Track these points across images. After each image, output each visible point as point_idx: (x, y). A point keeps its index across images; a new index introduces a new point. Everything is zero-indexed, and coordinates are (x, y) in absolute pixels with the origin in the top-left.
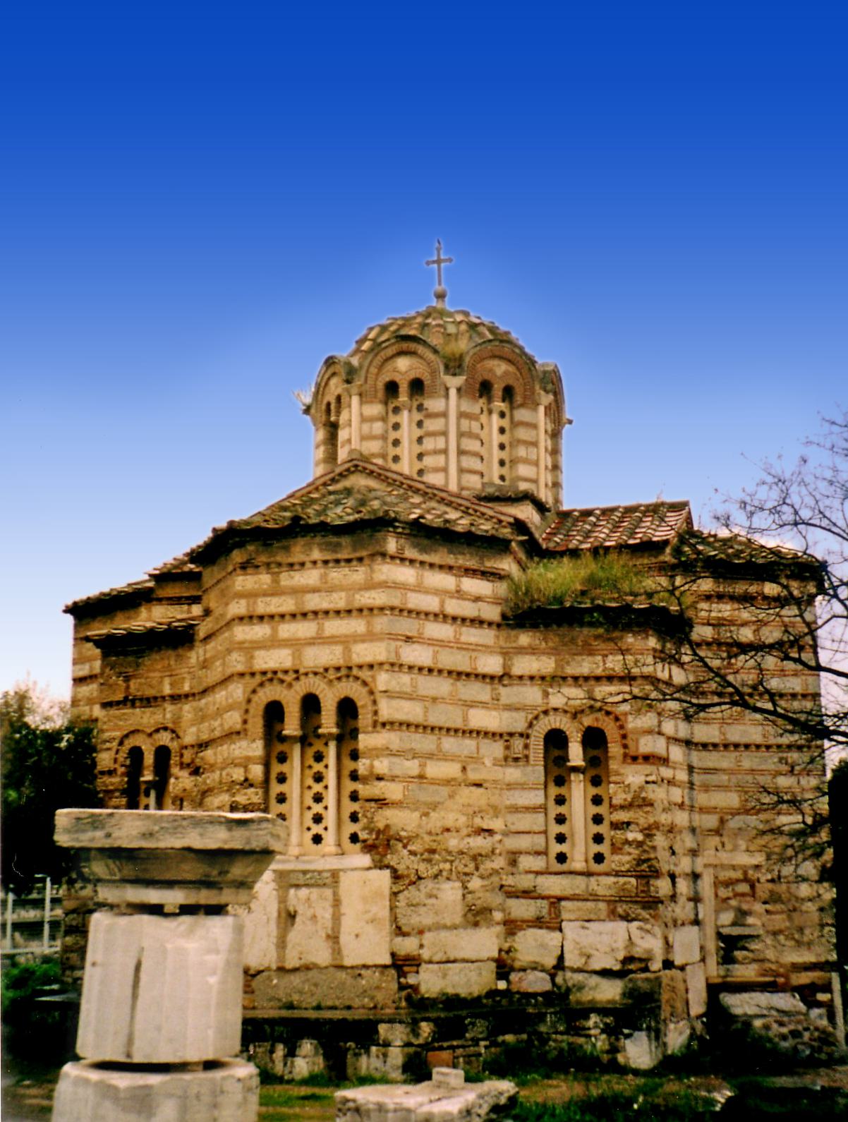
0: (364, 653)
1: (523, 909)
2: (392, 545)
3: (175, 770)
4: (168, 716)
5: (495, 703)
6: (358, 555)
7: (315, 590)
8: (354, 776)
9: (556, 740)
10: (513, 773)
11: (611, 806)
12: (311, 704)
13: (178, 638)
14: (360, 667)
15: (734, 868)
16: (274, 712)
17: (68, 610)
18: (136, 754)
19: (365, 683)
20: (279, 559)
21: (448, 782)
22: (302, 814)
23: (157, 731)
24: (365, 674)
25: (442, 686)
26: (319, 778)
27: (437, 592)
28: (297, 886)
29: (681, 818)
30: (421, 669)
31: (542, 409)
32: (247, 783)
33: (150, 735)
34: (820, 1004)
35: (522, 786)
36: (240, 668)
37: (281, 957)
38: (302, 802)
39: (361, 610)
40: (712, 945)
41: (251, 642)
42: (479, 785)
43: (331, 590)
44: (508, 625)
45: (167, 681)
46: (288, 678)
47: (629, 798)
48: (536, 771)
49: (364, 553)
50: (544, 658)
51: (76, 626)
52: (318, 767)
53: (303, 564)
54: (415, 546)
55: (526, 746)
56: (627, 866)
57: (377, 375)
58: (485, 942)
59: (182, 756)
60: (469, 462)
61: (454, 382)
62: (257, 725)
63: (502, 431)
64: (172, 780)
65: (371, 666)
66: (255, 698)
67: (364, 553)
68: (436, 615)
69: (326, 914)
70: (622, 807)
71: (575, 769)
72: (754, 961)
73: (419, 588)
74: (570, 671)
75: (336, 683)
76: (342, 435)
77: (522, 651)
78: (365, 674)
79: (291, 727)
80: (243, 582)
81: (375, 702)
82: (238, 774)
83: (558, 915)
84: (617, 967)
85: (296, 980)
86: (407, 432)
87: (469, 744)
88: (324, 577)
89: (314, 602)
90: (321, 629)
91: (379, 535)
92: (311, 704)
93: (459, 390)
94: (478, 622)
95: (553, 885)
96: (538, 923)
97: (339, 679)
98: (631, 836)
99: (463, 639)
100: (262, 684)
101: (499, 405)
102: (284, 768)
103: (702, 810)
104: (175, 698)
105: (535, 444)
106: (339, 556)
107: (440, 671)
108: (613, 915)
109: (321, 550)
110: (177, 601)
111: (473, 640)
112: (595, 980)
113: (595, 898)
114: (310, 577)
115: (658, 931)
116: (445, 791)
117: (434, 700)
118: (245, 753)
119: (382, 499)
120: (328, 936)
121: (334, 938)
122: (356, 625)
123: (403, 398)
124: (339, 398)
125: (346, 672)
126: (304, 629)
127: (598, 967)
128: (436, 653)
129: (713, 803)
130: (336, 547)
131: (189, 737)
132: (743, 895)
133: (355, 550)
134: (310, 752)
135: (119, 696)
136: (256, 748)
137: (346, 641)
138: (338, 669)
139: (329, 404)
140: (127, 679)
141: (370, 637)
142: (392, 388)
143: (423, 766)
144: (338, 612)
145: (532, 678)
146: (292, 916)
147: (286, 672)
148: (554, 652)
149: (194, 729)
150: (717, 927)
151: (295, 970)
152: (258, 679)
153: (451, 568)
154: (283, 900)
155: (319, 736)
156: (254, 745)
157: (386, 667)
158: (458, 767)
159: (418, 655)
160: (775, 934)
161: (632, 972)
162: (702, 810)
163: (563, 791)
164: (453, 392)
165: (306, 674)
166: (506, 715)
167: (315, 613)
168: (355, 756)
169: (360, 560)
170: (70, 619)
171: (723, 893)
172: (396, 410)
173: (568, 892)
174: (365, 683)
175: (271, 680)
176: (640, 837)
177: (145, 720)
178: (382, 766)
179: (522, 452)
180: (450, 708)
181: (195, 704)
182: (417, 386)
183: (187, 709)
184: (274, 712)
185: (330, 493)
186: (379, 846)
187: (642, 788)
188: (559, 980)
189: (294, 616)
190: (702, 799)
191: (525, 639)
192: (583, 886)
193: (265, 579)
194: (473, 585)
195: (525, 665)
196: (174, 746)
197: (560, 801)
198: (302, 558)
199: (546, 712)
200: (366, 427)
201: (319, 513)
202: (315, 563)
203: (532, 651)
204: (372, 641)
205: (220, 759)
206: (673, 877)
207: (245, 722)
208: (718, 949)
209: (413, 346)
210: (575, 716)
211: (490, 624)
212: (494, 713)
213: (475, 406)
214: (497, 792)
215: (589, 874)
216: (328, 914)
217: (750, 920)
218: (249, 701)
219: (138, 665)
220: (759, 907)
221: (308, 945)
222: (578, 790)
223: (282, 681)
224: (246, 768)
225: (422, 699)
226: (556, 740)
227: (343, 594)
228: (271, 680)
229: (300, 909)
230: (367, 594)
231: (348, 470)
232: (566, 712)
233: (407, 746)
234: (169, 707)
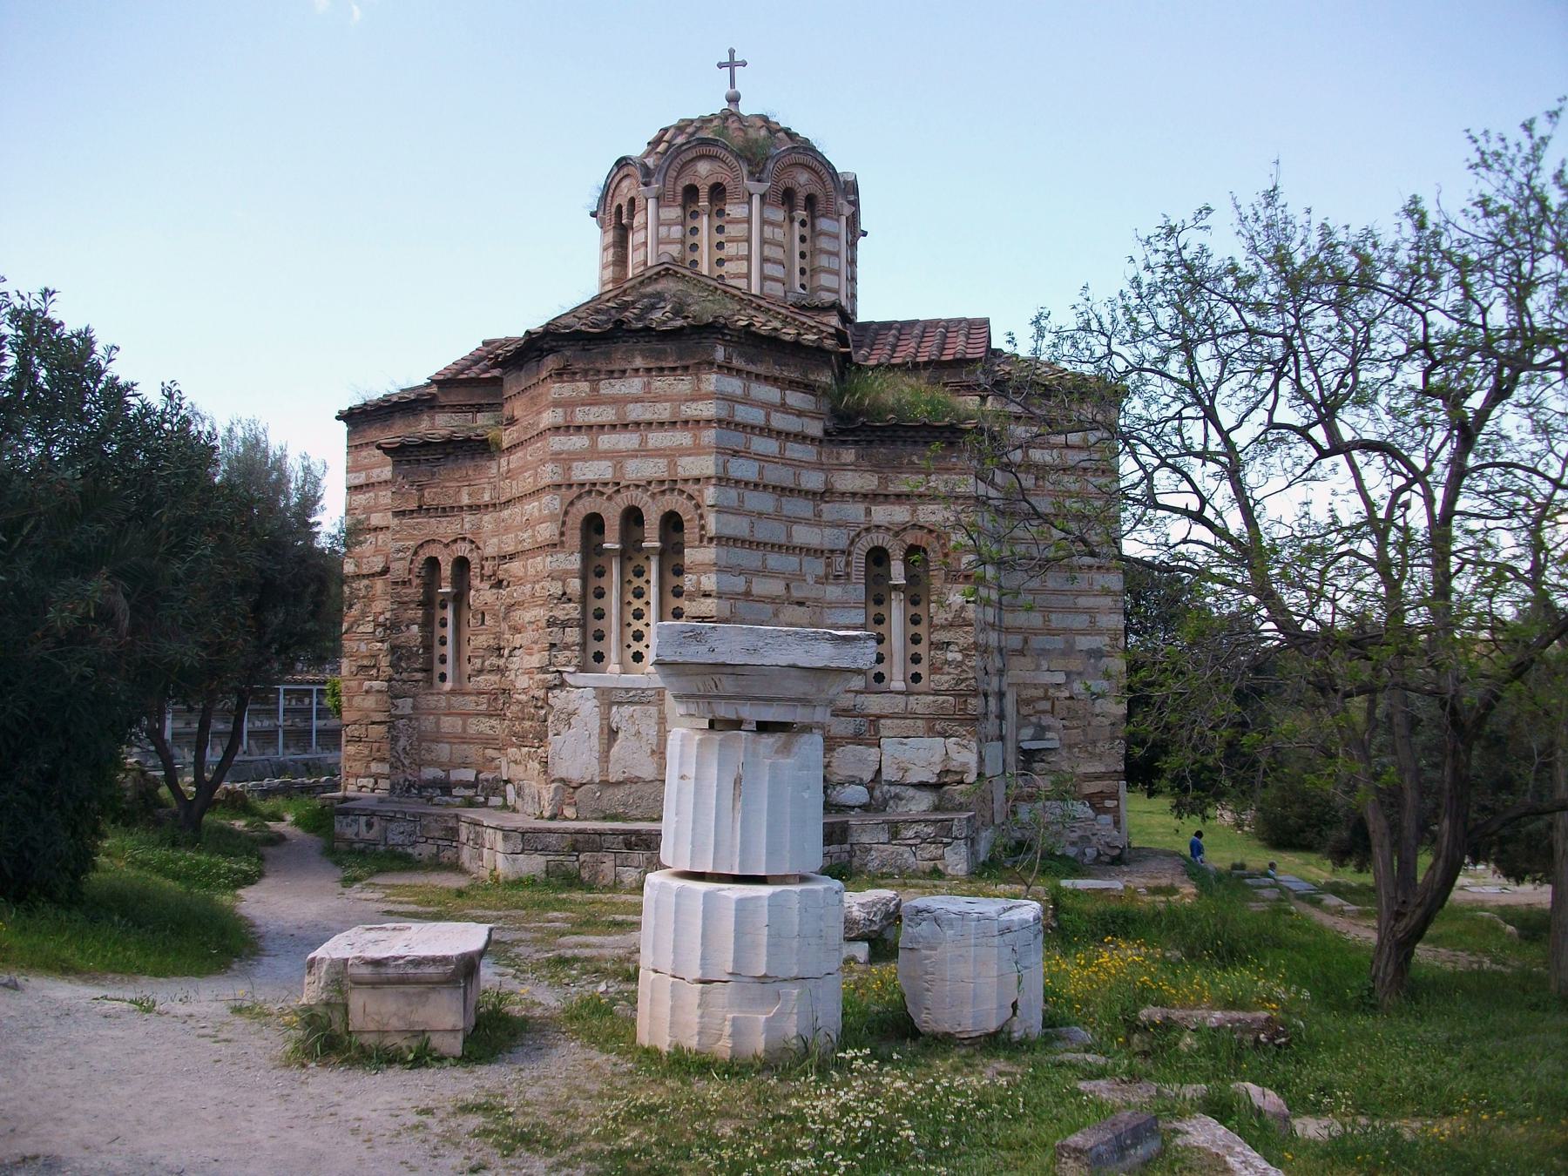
0: (693, 466)
1: (842, 727)
2: (720, 354)
3: (476, 582)
4: (467, 526)
5: (817, 521)
6: (684, 363)
7: (638, 400)
8: (678, 592)
9: (878, 557)
10: (833, 592)
11: (931, 625)
12: (633, 517)
13: (481, 448)
14: (686, 481)
15: (1036, 686)
16: (594, 524)
17: (342, 417)
18: (433, 563)
19: (691, 497)
20: (598, 365)
21: (773, 600)
22: (622, 632)
23: (455, 541)
24: (691, 488)
26: (639, 594)
27: (764, 405)
28: (620, 704)
29: (993, 638)
30: (747, 484)
31: (843, 219)
32: (565, 597)
33: (447, 545)
34: (1106, 811)
35: (843, 605)
36: (558, 479)
37: (605, 770)
38: (621, 619)
39: (686, 422)
40: (1011, 759)
41: (569, 453)
42: (801, 604)
43: (656, 400)
44: (831, 441)
45: (465, 491)
46: (609, 490)
47: (950, 617)
48: (858, 591)
49: (690, 362)
50: (867, 475)
51: (349, 433)
52: (638, 582)
53: (624, 372)
54: (740, 355)
55: (848, 564)
56: (946, 686)
57: (676, 178)
59: (482, 568)
60: (771, 269)
61: (758, 188)
62: (574, 538)
63: (803, 239)
64: (472, 593)
65: (697, 480)
66: (573, 510)
67: (690, 362)
68: (761, 429)
69: (651, 731)
70: (943, 627)
71: (896, 588)
72: (1051, 772)
73: (746, 400)
74: (892, 489)
75: (659, 497)
76: (635, 239)
77: (843, 467)
78: (691, 488)
79: (611, 543)
80: (558, 390)
81: (701, 517)
82: (556, 588)
83: (877, 731)
84: (934, 780)
85: (620, 793)
87: (792, 562)
88: (647, 385)
89: (635, 412)
90: (644, 441)
91: (706, 343)
92: (633, 517)
93: (763, 197)
94: (801, 438)
95: (874, 704)
96: (857, 739)
97: (663, 492)
98: (950, 656)
99: (788, 454)
100: (579, 497)
101: (801, 214)
102: (603, 582)
103: (1008, 630)
104: (474, 508)
105: (837, 254)
106: (664, 364)
107: (765, 487)
108: (931, 732)
109: (644, 357)
110: (457, 408)
111: (796, 456)
112: (911, 792)
113: (914, 716)
114: (634, 385)
115: (974, 745)
116: (769, 608)
117: (760, 514)
118: (563, 566)
119: (704, 308)
120: (653, 752)
122: (683, 438)
123: (703, 203)
124: (632, 201)
125: (671, 485)
127: (915, 781)
128: (761, 469)
129: (1017, 624)
130: (660, 354)
131: (489, 551)
132: (1044, 712)
133: (681, 359)
134: (630, 567)
135: (413, 506)
136: (575, 562)
137: (671, 454)
138: (662, 482)
139: (620, 207)
140: (421, 488)
141: (696, 450)
142: (691, 192)
143: (749, 582)
144: (662, 424)
145: (854, 494)
146: (612, 734)
147: (606, 484)
148: (877, 468)
149: (495, 540)
150: (1018, 742)
151: (619, 783)
152: (575, 491)
153: (776, 379)
154: (606, 717)
155: (641, 549)
156: (572, 558)
157: (713, 481)
158: (782, 584)
159: (744, 469)
160: (1070, 747)
161: (945, 784)
162: (1008, 630)
163: (882, 610)
164: (756, 200)
165: (628, 487)
166: (827, 531)
167: (638, 424)
168: (679, 571)
169: (686, 368)
170: (342, 426)
171: (1025, 711)
172: (695, 215)
173: (885, 712)
174: (691, 497)
175: (590, 492)
176: (959, 657)
177: (441, 531)
178: (709, 582)
179: (824, 261)
180: (776, 523)
181: (496, 515)
182: (718, 192)
183: (488, 519)
184: (594, 524)
185: (644, 296)
187: (963, 608)
188: (877, 793)
189: (614, 426)
190: (1009, 619)
191: (849, 455)
192: (902, 706)
193: (584, 387)
194: (795, 399)
196: (474, 558)
197: (879, 620)
198: (624, 365)
199: (868, 530)
200: (663, 231)
201: (639, 318)
202: (637, 370)
203: (856, 467)
204: (698, 454)
205: (531, 571)
206: (986, 695)
207: (562, 534)
208: (1018, 761)
209: (714, 150)
210: (897, 534)
211: (813, 439)
212: (816, 530)
213: (779, 215)
214: (818, 610)
215: (907, 693)
216: (653, 731)
217: (1049, 735)
218: (566, 513)
219: (433, 474)
220: (1059, 724)
222: (897, 611)
223: (602, 494)
224: (564, 582)
225: (749, 514)
226: (878, 557)
227: (668, 405)
228: (590, 492)
229: (623, 725)
230: (694, 406)
231: (658, 273)
232: (888, 529)
233: (733, 561)
234: (468, 518)
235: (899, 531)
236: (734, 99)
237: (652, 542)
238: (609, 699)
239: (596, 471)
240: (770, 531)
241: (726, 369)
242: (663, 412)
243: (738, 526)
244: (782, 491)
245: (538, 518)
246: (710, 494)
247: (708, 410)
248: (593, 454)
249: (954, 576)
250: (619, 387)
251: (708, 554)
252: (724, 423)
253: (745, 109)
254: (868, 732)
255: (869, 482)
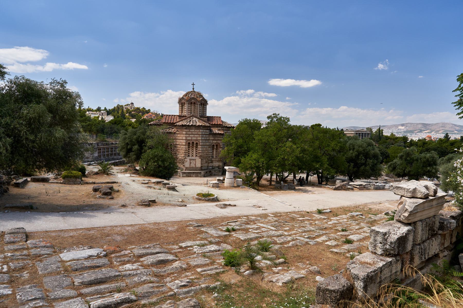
0: (199, 138)
10: (209, 149)
25: (204, 141)
58: (206, 165)
62: (187, 145)
86: (193, 108)
89: (193, 133)
92: (193, 143)
95: (213, 159)
96: (211, 163)
114: (193, 130)
121: (195, 165)
122: (198, 136)
125: (197, 140)
126: (193, 136)
136: (187, 147)
137: (197, 137)
141: (199, 137)
142: (191, 103)
146: (191, 163)
159: (203, 138)
178: (200, 149)
182: (194, 103)
184: (189, 143)
186: (200, 157)
194: (207, 131)
195: (211, 138)
221: (193, 165)
222: (215, 150)
226: (213, 145)
235: (215, 143)
236: (193, 89)
237: (195, 146)
238: (190, 160)
239: (190, 138)
240: (205, 144)
241: (202, 129)
242: (196, 133)
243: (203, 144)
244: (206, 140)
245: (184, 142)
246: (200, 141)
247: (200, 133)
248: (189, 137)
249: (220, 148)
250: (192, 130)
251: (200, 147)
252: (202, 134)
253: (195, 90)
254: (212, 162)
255: (213, 138)
